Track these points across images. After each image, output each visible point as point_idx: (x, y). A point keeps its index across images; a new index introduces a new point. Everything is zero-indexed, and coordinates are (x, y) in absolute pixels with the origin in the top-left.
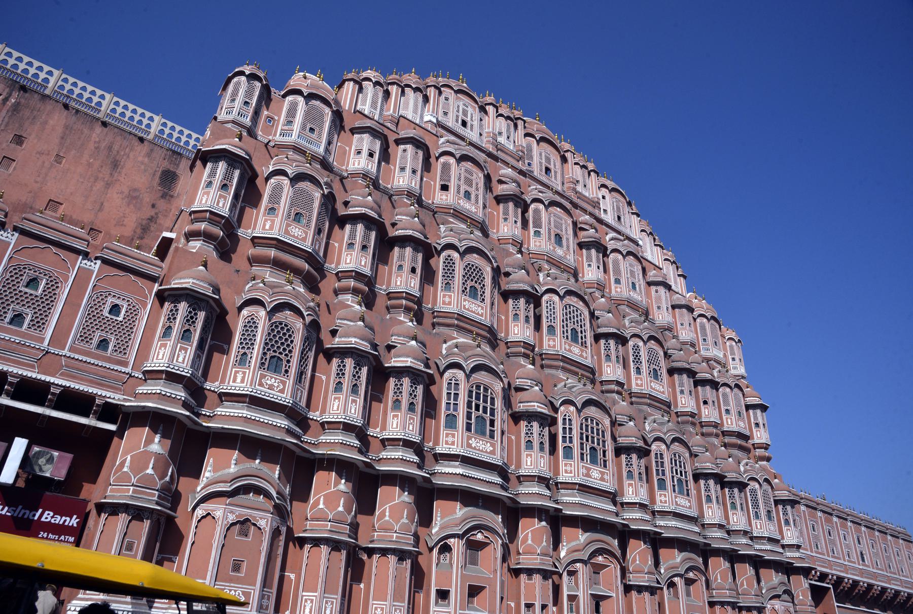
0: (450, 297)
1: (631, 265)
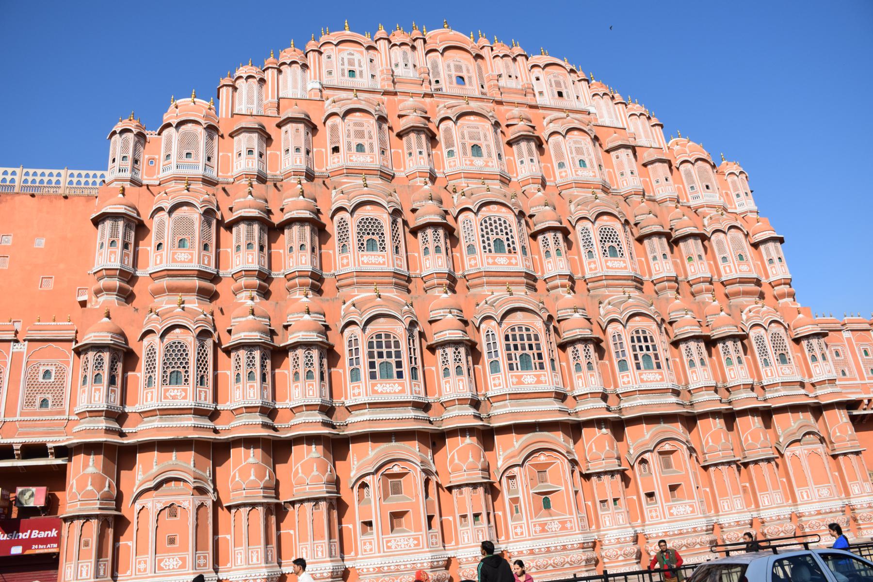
0: (347, 257)
1: (575, 142)
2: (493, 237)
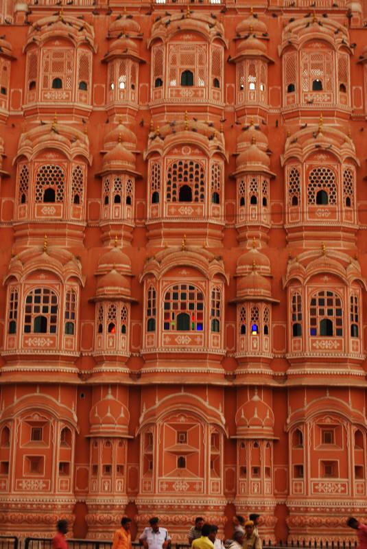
1: (313, 58)
2: (180, 183)
